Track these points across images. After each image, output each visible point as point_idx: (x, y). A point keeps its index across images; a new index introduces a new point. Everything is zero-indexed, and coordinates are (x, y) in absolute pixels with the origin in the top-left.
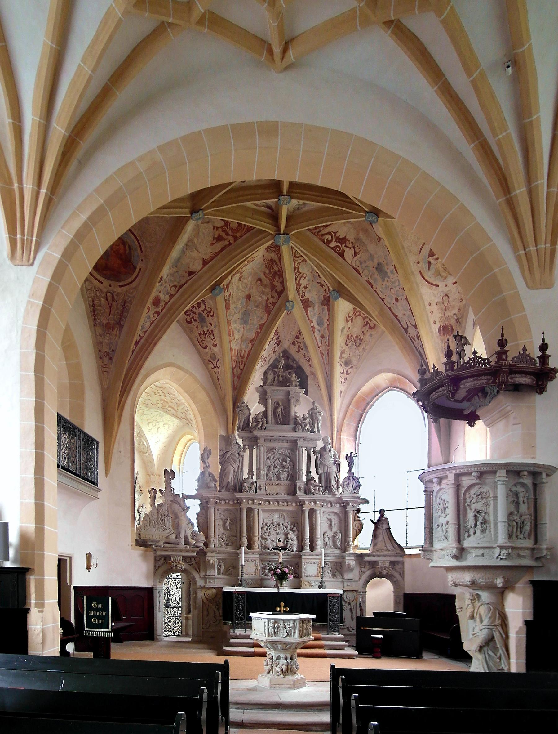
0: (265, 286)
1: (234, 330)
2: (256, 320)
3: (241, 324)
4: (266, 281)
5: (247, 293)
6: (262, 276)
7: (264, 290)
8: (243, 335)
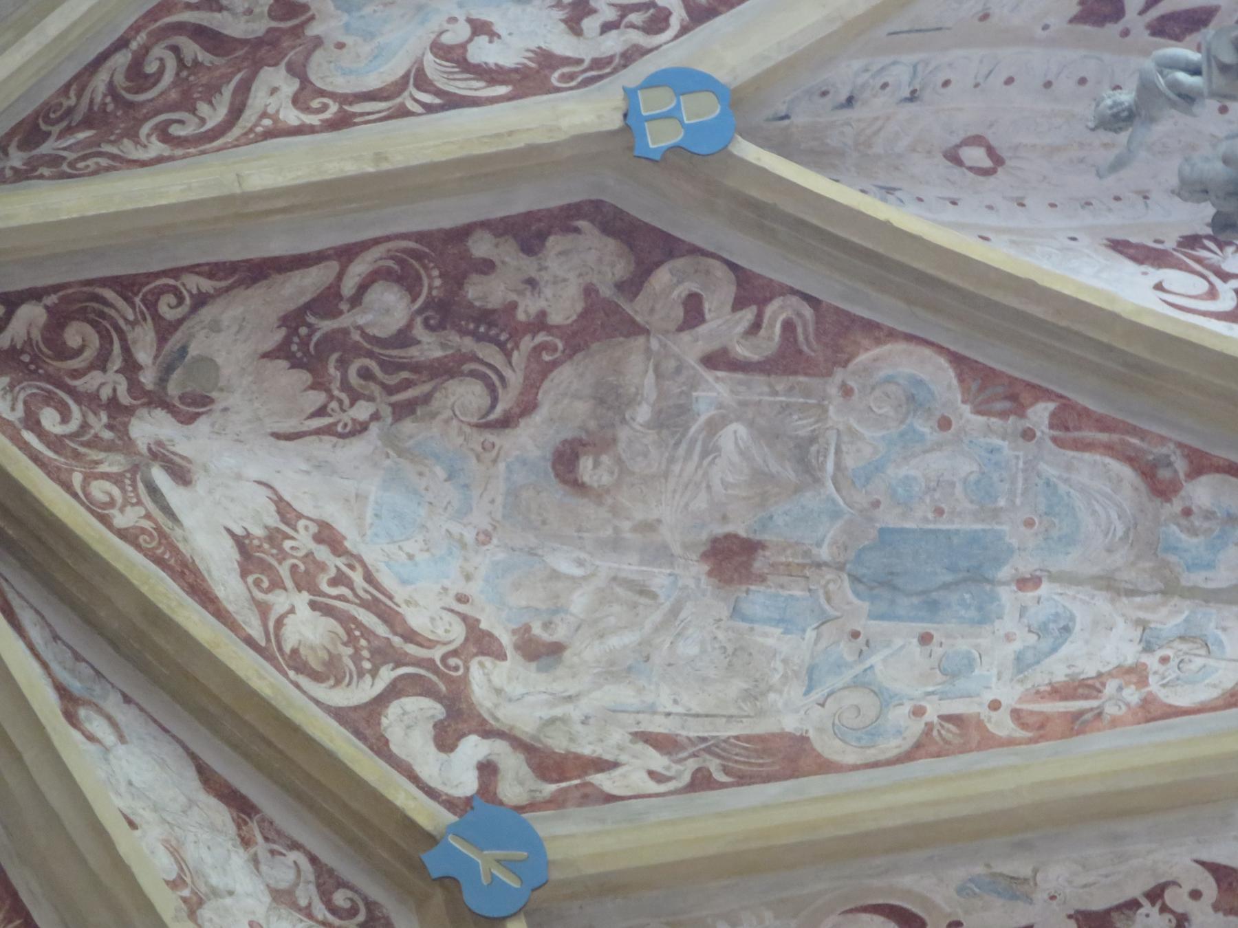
0: (611, 400)
1: (1040, 678)
2: (937, 463)
3: (985, 616)
4: (565, 401)
5: (695, 573)
6: (531, 440)
7: (643, 413)
8: (1109, 584)
